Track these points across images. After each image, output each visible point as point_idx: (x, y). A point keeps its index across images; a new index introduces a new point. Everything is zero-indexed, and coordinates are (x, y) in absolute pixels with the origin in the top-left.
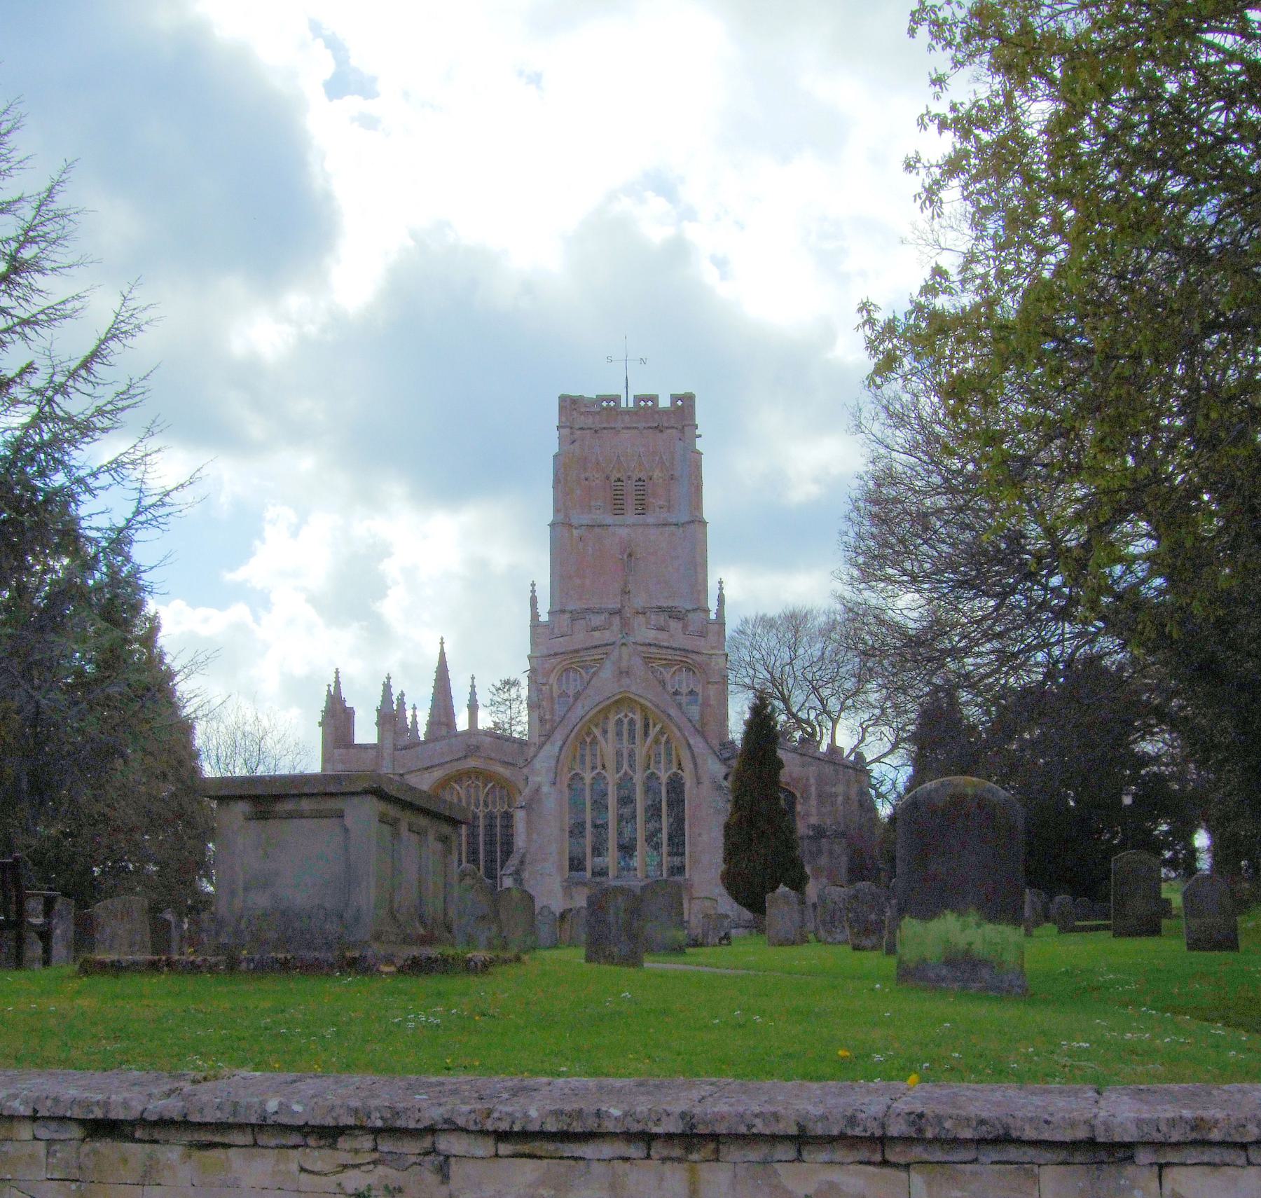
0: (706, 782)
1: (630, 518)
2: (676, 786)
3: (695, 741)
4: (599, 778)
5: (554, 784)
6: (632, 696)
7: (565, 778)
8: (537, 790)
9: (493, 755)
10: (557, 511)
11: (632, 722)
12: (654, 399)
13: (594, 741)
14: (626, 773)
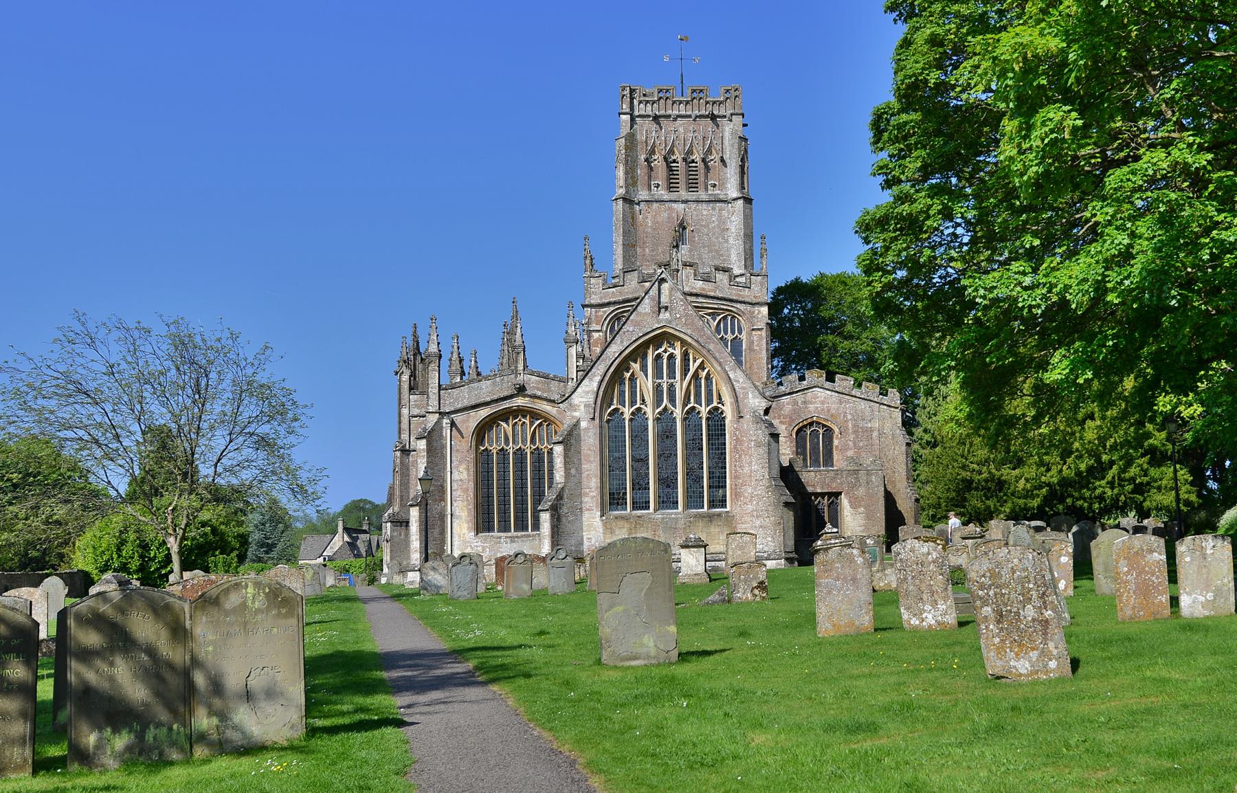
1: (683, 194)
2: (717, 420)
3: (737, 376)
5: (593, 419)
8: (576, 425)
9: (539, 393)
11: (671, 357)
13: (633, 379)
14: (665, 409)
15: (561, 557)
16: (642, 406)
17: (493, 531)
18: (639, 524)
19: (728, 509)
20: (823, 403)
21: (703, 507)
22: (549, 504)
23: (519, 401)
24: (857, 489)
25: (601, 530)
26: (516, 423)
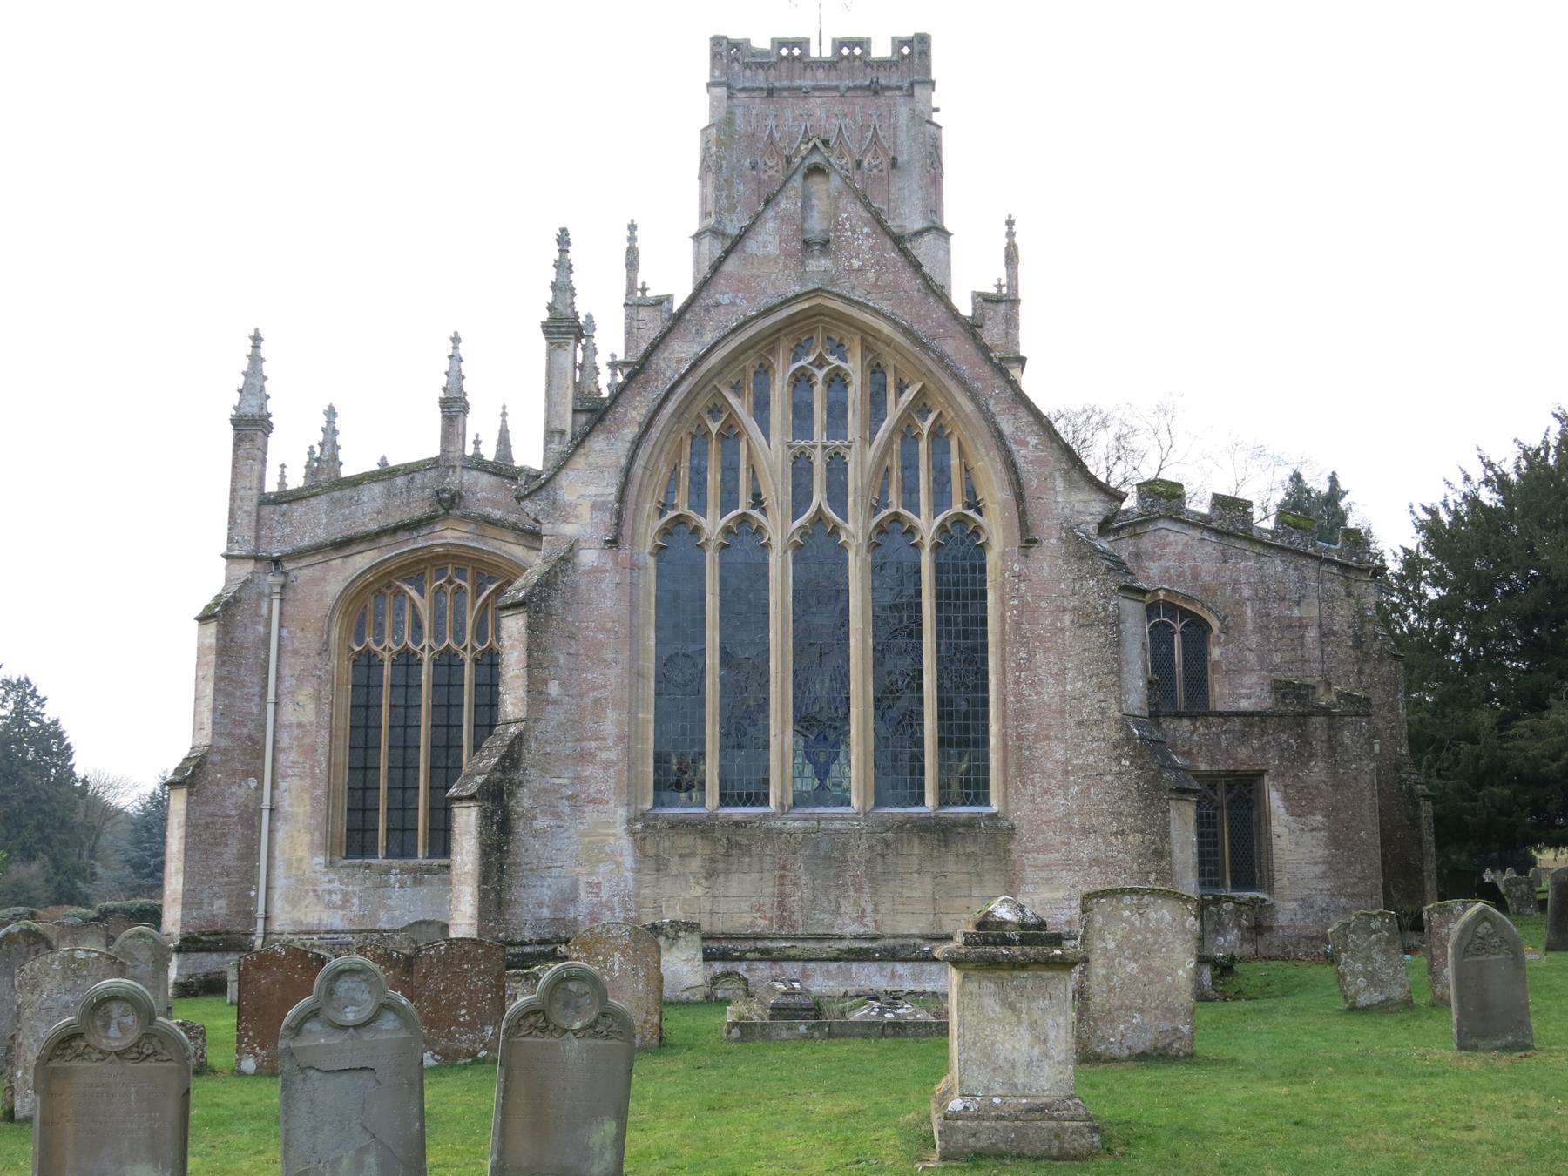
0: (1051, 541)
4: (744, 532)
6: (838, 305)
7: (648, 528)
9: (497, 514)
10: (705, 214)
11: (837, 380)
15: (350, 1015)
16: (752, 512)
17: (375, 855)
18: (738, 844)
19: (995, 807)
20: (1180, 557)
21: (920, 801)
22: (479, 779)
23: (449, 533)
24: (1305, 764)
25: (628, 861)
26: (441, 586)
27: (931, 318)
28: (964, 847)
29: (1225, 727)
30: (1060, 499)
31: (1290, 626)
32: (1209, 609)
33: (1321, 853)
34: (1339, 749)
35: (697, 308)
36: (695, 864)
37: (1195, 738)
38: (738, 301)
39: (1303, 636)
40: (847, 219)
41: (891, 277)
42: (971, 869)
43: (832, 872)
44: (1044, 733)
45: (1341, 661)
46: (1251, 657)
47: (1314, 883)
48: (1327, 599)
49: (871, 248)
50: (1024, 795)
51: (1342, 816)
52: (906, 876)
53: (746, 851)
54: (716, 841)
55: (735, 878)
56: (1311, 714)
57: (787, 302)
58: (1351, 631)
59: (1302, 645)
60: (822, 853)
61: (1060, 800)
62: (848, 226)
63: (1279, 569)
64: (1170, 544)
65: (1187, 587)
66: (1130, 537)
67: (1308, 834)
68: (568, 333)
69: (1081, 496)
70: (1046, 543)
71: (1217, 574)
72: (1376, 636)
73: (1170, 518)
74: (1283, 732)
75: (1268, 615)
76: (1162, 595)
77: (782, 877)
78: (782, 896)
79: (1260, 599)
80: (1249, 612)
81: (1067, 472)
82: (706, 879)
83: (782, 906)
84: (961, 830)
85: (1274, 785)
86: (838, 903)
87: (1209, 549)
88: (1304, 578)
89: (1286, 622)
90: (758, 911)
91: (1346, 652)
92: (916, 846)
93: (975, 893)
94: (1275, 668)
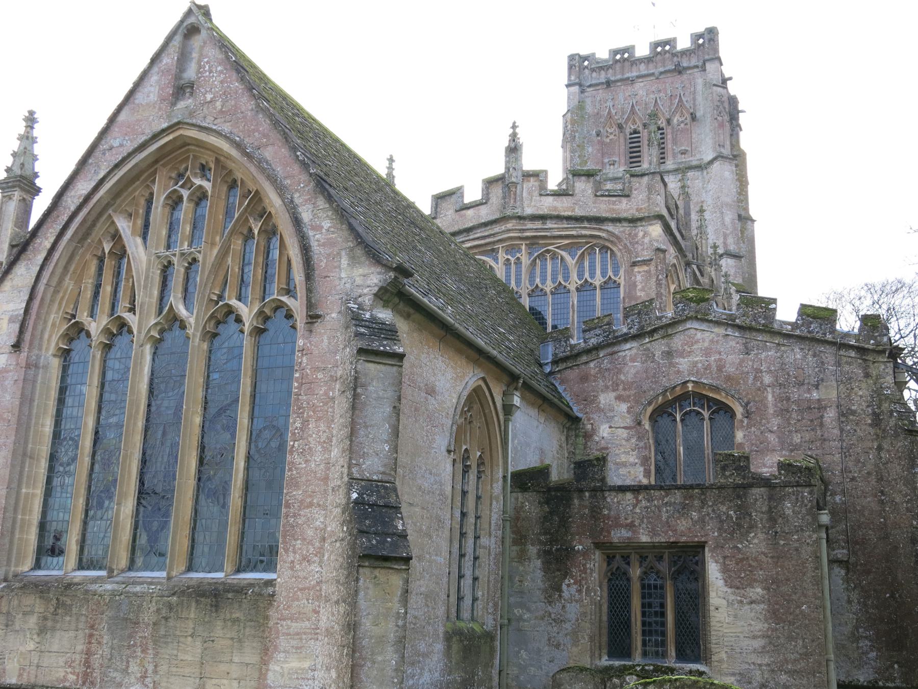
0: (333, 316)
6: (193, 133)
12: (671, 42)
18: (64, 604)
20: (707, 352)
24: (744, 535)
27: (258, 131)
28: (231, 613)
29: (666, 500)
30: (343, 275)
31: (810, 408)
32: (733, 396)
33: (760, 626)
34: (780, 520)
35: (97, 153)
36: (33, 620)
37: (638, 510)
38: (125, 142)
39: (822, 417)
40: (207, 62)
41: (233, 102)
42: (234, 634)
43: (127, 632)
44: (308, 500)
45: (861, 439)
46: (772, 438)
47: (753, 658)
48: (846, 381)
49: (222, 82)
50: (285, 562)
51: (784, 589)
52: (182, 639)
53: (68, 609)
54: (48, 600)
55: (58, 634)
56: (751, 486)
57: (155, 137)
58: (870, 410)
59: (822, 425)
60: (122, 615)
61: (315, 567)
62: (207, 68)
63: (798, 356)
64: (697, 342)
65: (713, 378)
66: (663, 338)
67: (747, 607)
68: (14, 187)
69: (361, 271)
70: (328, 318)
71: (740, 364)
72: (891, 412)
73: (696, 318)
74: (723, 503)
75: (788, 399)
76: (690, 386)
77: (91, 636)
78: (89, 653)
79: (780, 385)
80: (770, 397)
81: (352, 249)
82: (38, 635)
83: (87, 664)
84: (230, 595)
85: (712, 557)
86: (128, 662)
87: (733, 343)
88: (823, 363)
89: (806, 405)
90: (70, 666)
91: (865, 429)
92: (193, 609)
93: (236, 659)
94: (795, 448)
